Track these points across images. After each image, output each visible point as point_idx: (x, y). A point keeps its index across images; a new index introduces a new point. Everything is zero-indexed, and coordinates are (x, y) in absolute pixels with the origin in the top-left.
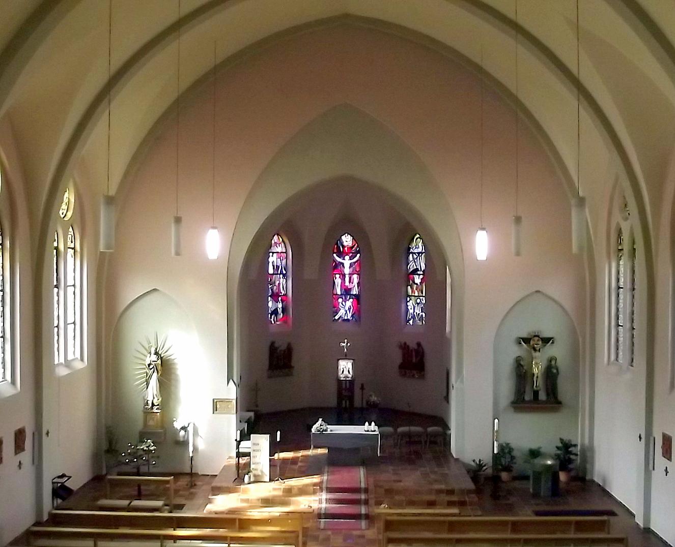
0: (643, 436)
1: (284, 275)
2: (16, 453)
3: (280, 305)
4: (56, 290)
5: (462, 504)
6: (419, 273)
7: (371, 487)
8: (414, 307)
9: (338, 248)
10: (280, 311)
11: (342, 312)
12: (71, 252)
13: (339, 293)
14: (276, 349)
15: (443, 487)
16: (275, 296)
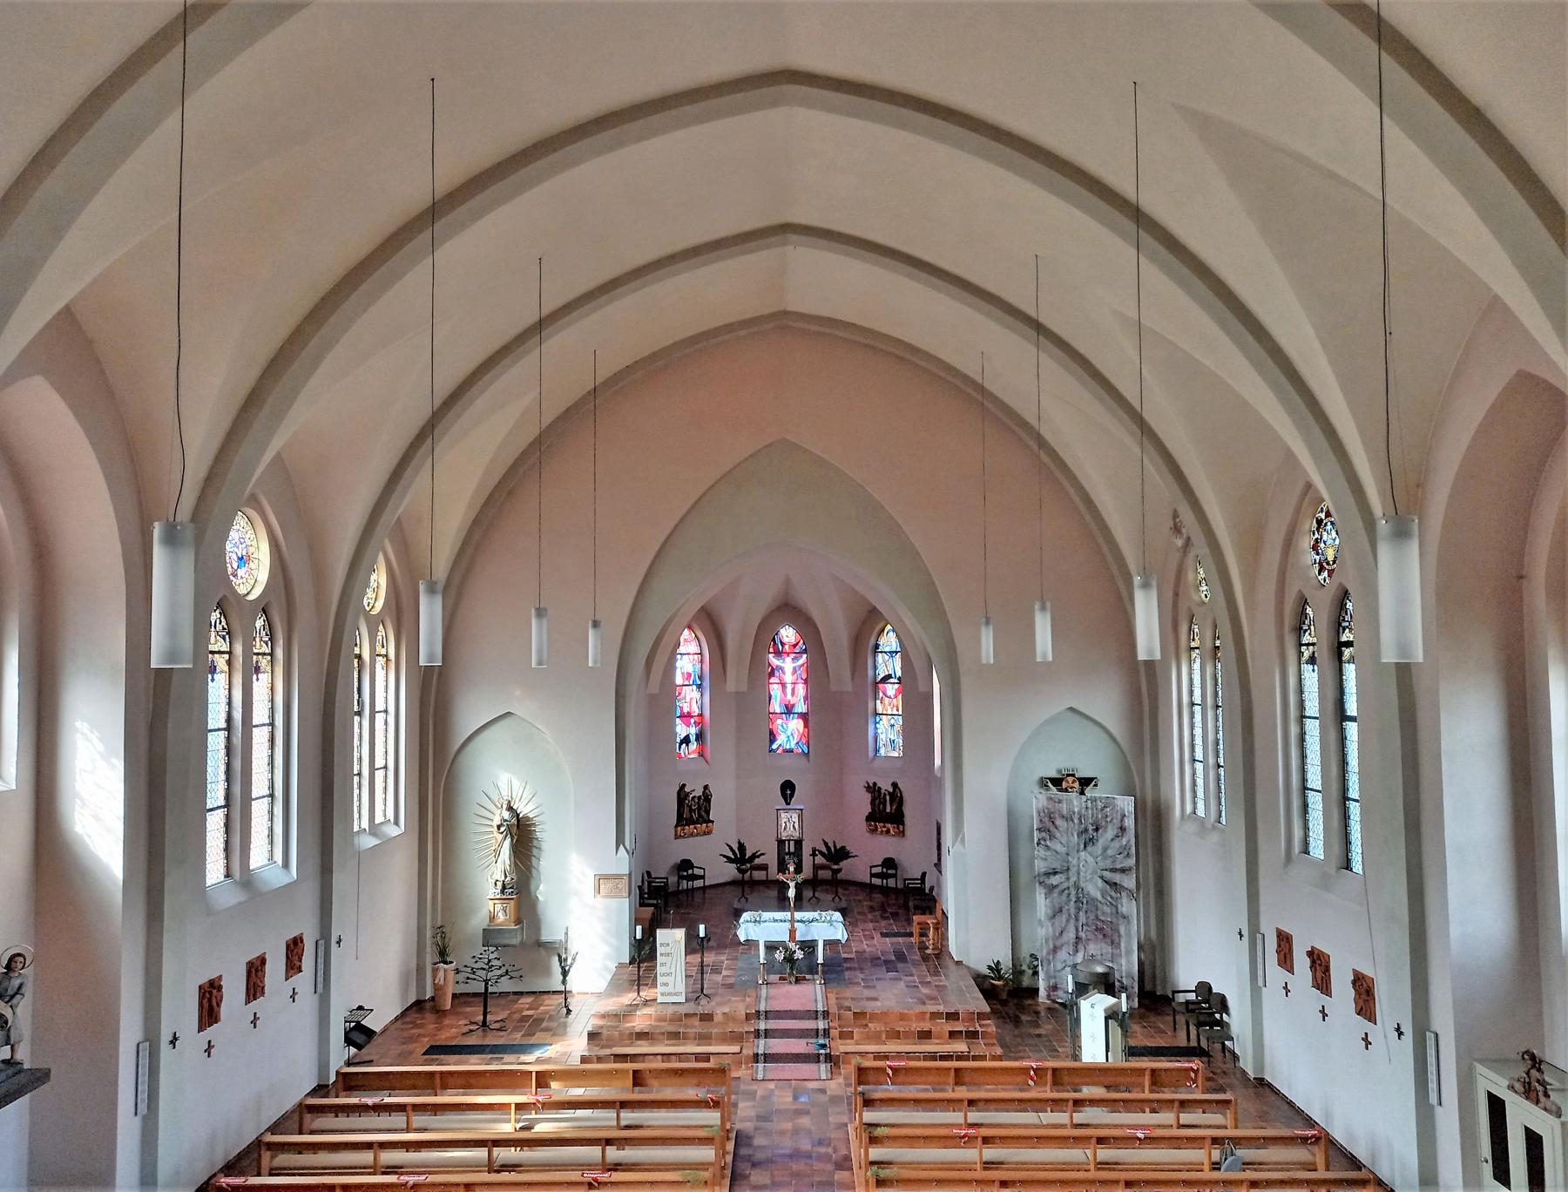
0: (1245, 933)
1: (699, 686)
2: (248, 1002)
3: (693, 731)
4: (357, 718)
5: (972, 1035)
7: (833, 1010)
8: (888, 731)
10: (693, 738)
11: (781, 740)
12: (380, 661)
14: (687, 794)
15: (941, 1008)
16: (686, 717)
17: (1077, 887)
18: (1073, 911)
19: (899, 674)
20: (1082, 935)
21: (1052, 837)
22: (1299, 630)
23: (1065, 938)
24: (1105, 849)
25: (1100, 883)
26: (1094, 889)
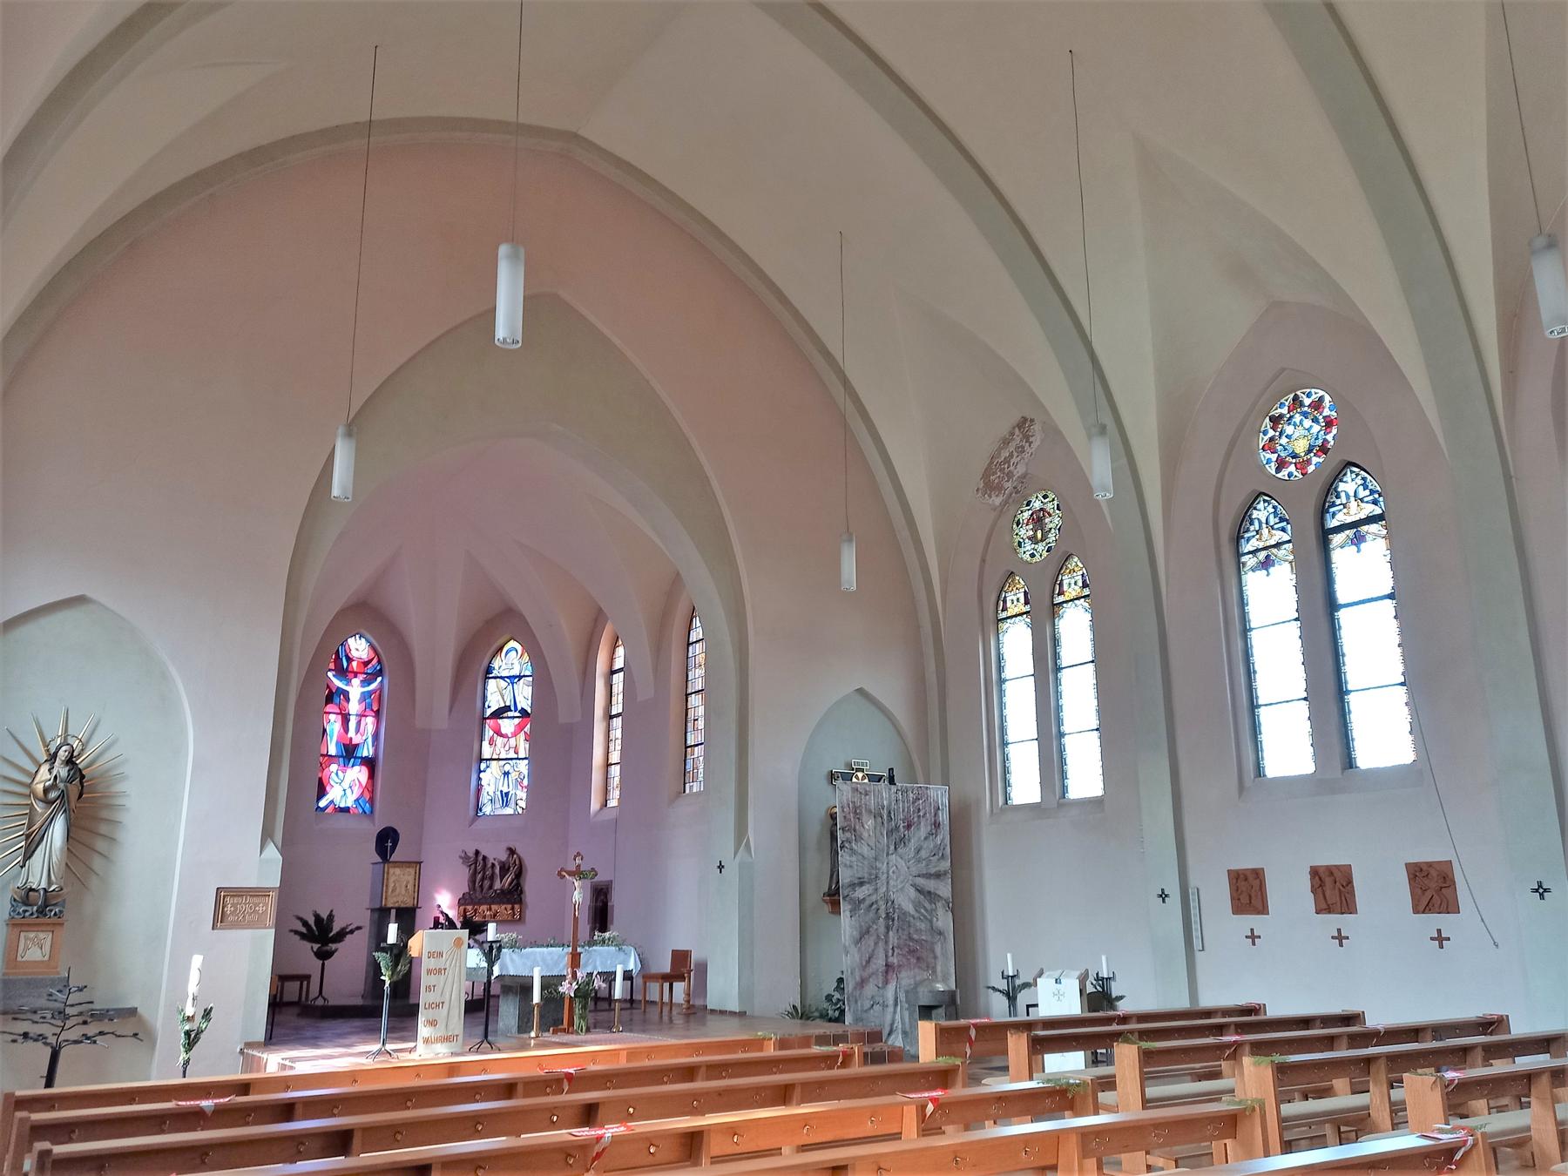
6: (510, 714)
9: (338, 659)
13: (333, 751)
17: (890, 902)
18: (882, 930)
19: (525, 703)
20: (894, 960)
21: (859, 838)
22: (1237, 538)
23: (873, 967)
24: (918, 851)
25: (912, 891)
26: (906, 900)
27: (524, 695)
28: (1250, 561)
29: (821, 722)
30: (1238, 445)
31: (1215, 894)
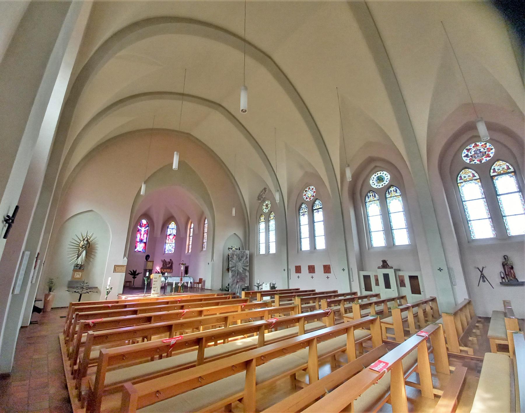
8: (170, 247)
13: (138, 240)
17: (238, 270)
22: (299, 210)
26: (241, 270)
27: (174, 232)
28: (301, 214)
29: (227, 239)
30: (300, 195)
31: (293, 270)
